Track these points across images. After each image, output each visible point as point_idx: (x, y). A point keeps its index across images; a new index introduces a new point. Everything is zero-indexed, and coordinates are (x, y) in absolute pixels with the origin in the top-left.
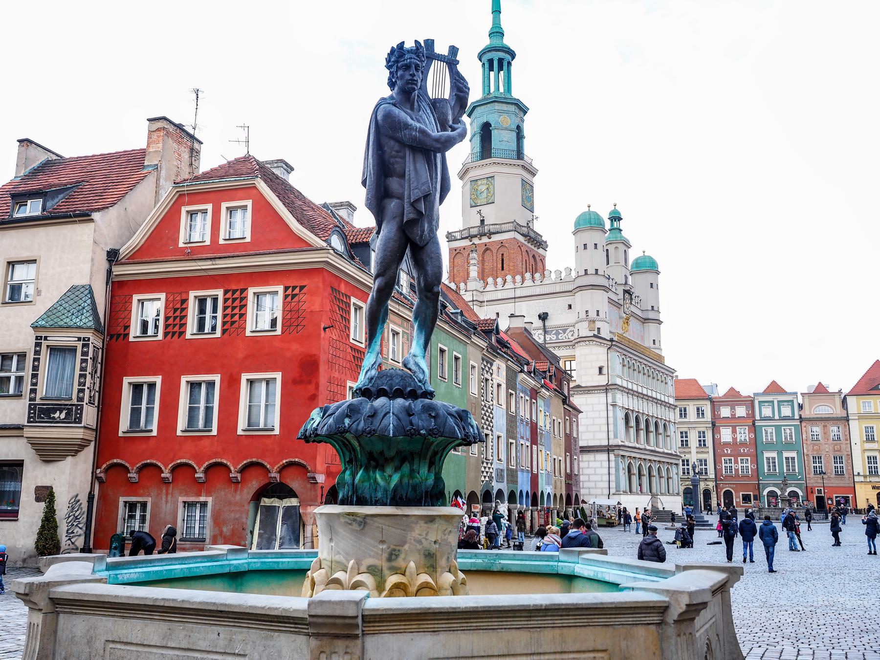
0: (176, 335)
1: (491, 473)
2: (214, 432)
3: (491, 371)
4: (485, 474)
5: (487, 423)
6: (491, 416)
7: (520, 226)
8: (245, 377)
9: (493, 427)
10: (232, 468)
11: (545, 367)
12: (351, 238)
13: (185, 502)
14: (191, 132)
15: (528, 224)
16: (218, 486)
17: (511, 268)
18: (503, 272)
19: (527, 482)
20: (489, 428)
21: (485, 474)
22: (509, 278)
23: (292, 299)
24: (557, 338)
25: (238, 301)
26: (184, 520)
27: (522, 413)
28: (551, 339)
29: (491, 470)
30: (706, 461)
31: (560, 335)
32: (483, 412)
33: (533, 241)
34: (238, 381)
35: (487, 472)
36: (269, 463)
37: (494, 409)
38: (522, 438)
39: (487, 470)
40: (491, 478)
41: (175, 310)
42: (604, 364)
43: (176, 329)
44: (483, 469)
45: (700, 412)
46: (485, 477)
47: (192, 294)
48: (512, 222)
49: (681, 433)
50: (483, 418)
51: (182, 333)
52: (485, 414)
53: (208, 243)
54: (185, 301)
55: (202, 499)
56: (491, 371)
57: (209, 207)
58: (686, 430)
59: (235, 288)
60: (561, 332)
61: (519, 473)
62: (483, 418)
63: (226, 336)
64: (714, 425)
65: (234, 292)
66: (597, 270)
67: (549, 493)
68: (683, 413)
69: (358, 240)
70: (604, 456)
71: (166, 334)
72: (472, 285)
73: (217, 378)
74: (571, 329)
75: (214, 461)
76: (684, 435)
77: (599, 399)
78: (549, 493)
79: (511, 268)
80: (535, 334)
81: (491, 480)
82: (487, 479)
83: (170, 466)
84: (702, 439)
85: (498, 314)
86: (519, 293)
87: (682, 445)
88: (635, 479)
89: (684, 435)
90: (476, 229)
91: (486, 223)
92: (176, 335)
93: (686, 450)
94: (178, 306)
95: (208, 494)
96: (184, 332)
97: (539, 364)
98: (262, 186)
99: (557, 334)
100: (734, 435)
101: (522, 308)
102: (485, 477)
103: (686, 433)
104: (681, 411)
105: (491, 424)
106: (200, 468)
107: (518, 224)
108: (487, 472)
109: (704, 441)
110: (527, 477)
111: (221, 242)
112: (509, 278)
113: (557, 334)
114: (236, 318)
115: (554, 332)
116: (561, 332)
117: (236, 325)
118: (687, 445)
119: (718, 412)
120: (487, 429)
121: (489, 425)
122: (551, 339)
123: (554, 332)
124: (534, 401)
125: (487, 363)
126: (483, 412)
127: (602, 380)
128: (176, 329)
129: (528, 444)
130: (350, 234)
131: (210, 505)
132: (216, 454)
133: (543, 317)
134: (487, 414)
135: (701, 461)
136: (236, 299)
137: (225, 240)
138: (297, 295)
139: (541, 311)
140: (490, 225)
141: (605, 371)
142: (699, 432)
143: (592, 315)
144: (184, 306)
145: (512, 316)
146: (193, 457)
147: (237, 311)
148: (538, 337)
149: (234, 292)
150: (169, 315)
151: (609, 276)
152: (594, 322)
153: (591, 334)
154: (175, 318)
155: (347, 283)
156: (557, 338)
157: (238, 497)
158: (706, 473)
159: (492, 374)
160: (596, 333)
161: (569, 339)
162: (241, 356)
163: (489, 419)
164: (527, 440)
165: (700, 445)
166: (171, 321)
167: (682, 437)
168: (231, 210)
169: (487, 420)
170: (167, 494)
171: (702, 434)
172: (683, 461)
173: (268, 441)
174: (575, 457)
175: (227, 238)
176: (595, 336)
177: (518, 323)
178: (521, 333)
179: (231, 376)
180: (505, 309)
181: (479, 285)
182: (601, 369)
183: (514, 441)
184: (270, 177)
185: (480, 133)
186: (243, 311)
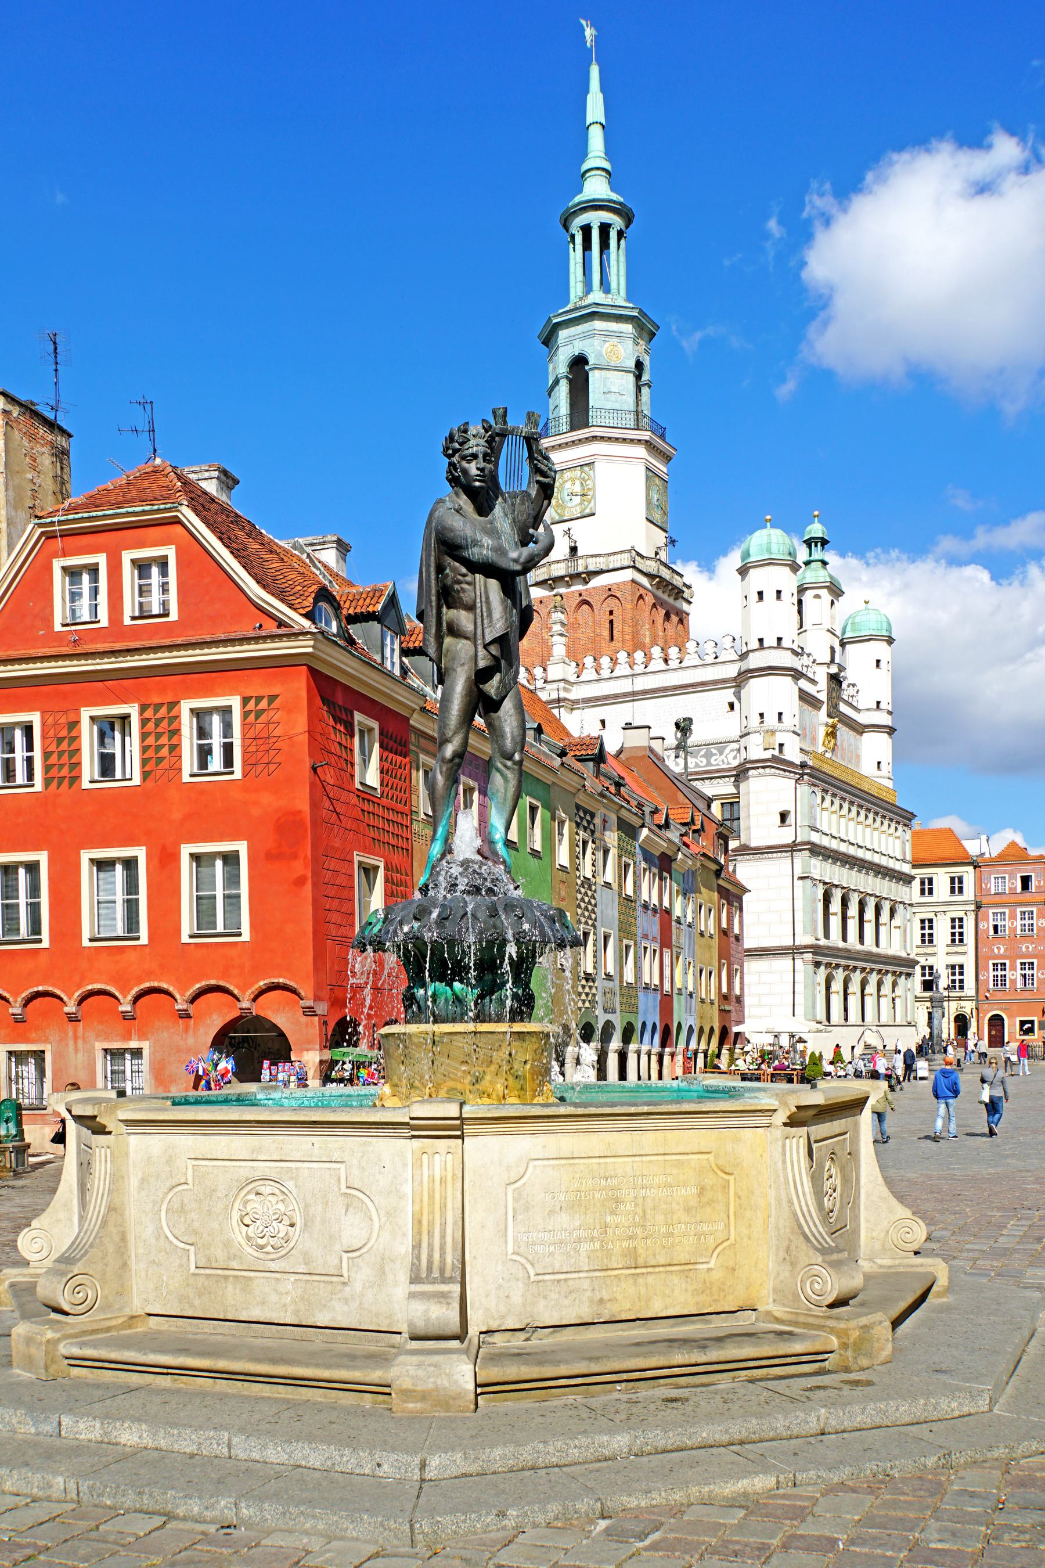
0: (66, 782)
1: (594, 995)
2: (144, 940)
3: (592, 827)
4: (583, 997)
5: (586, 914)
6: (593, 902)
7: (642, 557)
8: (186, 850)
9: (595, 920)
10: (177, 996)
11: (686, 816)
12: (347, 605)
13: (106, 1050)
14: (50, 415)
15: (657, 553)
16: (157, 1024)
17: (628, 637)
18: (612, 645)
19: (654, 1007)
20: (590, 922)
21: (583, 997)
22: (622, 656)
23: (257, 718)
24: (709, 764)
25: (164, 724)
26: (106, 1077)
27: (645, 896)
28: (697, 765)
29: (594, 991)
30: (961, 967)
31: (713, 758)
32: (579, 896)
33: (667, 585)
34: (176, 857)
35: (587, 994)
36: (237, 987)
37: (598, 891)
38: (645, 937)
39: (587, 990)
40: (593, 1003)
41: (60, 740)
42: (789, 806)
43: (64, 772)
44: (580, 989)
45: (956, 885)
46: (584, 1002)
47: (86, 713)
48: (629, 551)
49: (923, 921)
50: (579, 906)
51: (76, 778)
52: (583, 900)
53: (104, 623)
54: (75, 724)
55: (133, 1044)
56: (592, 827)
57: (101, 560)
58: (931, 916)
59: (156, 700)
60: (714, 751)
61: (641, 994)
62: (579, 906)
63: (150, 784)
64: (978, 907)
65: (158, 707)
66: (779, 639)
67: (691, 1026)
68: (927, 887)
69: (358, 610)
70: (785, 963)
71: (47, 781)
72: (555, 671)
73: (140, 853)
74: (735, 746)
75: (147, 985)
76: (927, 924)
77: (780, 867)
78: (691, 1026)
79: (628, 637)
80: (668, 757)
81: (594, 1007)
82: (587, 1004)
83: (77, 994)
84: (957, 930)
85: (603, 722)
86: (642, 684)
87: (923, 941)
88: (836, 1001)
89: (927, 924)
90: (562, 565)
91: (580, 553)
92: (66, 782)
93: (929, 950)
94: (64, 733)
95: (142, 1036)
96: (78, 777)
97: (676, 811)
98: (188, 515)
99: (708, 755)
100: (1012, 923)
101: (644, 711)
102: (584, 1002)
103: (931, 921)
104: (923, 883)
105: (593, 916)
106: (125, 997)
107: (638, 554)
108: (587, 994)
109: (961, 934)
110: (655, 999)
111: (127, 621)
112: (622, 656)
113: (708, 755)
114: (165, 751)
115: (702, 753)
116: (714, 751)
117: (165, 764)
118: (931, 941)
119: (986, 884)
120: (586, 923)
121: (590, 917)
122: (697, 765)
123: (702, 753)
124: (665, 874)
125: (585, 814)
126: (579, 896)
127: (785, 836)
128: (64, 772)
129: (656, 946)
130: (344, 598)
131: (146, 1053)
132: (149, 975)
133: (684, 727)
134: (586, 899)
135: (953, 967)
136: (162, 719)
137: (133, 618)
138: (263, 711)
139: (681, 715)
140: (588, 556)
141: (790, 820)
142: (953, 920)
143: (771, 720)
144: (73, 734)
145: (628, 727)
146: (113, 980)
147: (164, 740)
148: (675, 765)
149: (158, 707)
150: (49, 750)
151: (802, 649)
152: (773, 732)
153: (768, 755)
154: (61, 754)
155: (347, 688)
156: (709, 764)
157: (191, 1041)
158: (961, 988)
159: (593, 832)
160: (776, 753)
161: (728, 763)
162: (177, 815)
163: (590, 907)
164: (654, 939)
165: (953, 941)
166: (53, 760)
167: (923, 928)
168: (142, 567)
169: (586, 909)
170: (76, 1038)
171: (957, 923)
172: (923, 968)
173: (233, 952)
174: (736, 967)
175: (137, 614)
176: (774, 758)
177: (637, 739)
178: (643, 757)
179: (164, 848)
180: (618, 714)
181: (570, 672)
182: (783, 816)
183: (632, 943)
184: (201, 500)
185: (567, 377)
186: (174, 741)
